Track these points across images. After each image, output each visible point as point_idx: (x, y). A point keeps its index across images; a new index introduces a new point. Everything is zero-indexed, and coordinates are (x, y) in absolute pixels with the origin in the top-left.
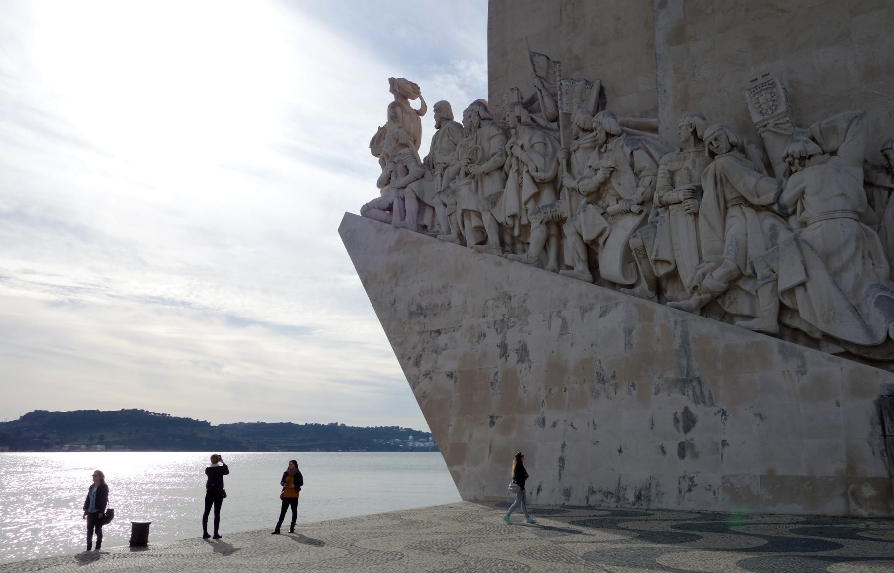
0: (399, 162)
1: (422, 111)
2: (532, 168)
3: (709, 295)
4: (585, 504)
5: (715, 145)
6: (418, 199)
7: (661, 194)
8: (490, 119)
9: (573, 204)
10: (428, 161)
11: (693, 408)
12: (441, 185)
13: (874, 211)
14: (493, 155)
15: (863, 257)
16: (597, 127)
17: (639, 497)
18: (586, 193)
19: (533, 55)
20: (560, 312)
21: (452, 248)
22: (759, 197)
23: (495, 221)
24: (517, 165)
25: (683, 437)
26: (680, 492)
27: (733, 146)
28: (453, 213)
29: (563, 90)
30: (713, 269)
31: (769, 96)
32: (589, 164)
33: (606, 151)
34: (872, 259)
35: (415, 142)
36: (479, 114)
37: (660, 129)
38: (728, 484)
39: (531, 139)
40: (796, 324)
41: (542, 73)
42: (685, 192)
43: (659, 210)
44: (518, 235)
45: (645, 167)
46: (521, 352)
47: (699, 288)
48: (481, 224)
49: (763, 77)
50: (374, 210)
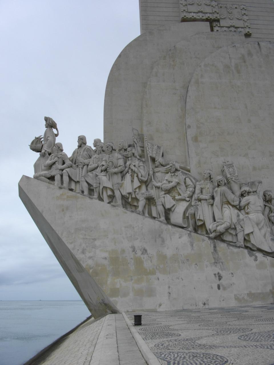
0: (60, 158)
1: (57, 135)
2: (140, 175)
4: (182, 309)
5: (221, 183)
6: (69, 177)
10: (72, 160)
11: (221, 272)
12: (82, 172)
14: (120, 166)
17: (204, 304)
18: (165, 190)
19: (133, 129)
20: (160, 235)
22: (233, 202)
24: (131, 172)
25: (218, 282)
26: (220, 301)
28: (98, 187)
29: (149, 147)
30: (221, 225)
33: (174, 176)
36: (112, 147)
37: (191, 171)
38: (237, 297)
39: (139, 164)
40: (248, 245)
43: (197, 201)
45: (190, 184)
47: (216, 231)
50: (42, 177)
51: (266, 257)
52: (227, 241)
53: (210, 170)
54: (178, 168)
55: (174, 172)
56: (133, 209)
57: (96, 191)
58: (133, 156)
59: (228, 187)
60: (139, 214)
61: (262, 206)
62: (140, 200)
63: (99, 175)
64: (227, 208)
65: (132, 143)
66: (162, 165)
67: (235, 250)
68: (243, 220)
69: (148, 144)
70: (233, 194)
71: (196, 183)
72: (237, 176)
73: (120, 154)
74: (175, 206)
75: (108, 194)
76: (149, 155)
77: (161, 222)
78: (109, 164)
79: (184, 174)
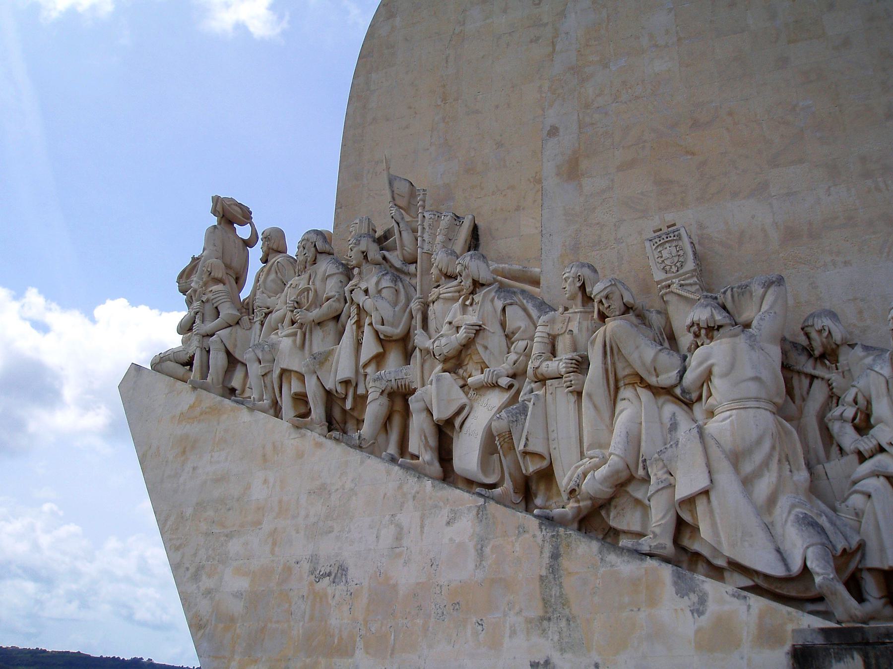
0: (208, 300)
3: (588, 503)
6: (228, 353)
8: (330, 254)
13: (794, 402)
14: (328, 299)
15: (779, 461)
16: (462, 273)
21: (266, 420)
23: (321, 388)
27: (628, 309)
28: (269, 372)
29: (426, 224)
30: (597, 467)
33: (471, 304)
34: (789, 464)
35: (237, 280)
36: (315, 245)
39: (377, 283)
40: (696, 547)
41: (402, 202)
43: (533, 385)
44: (350, 409)
45: (520, 328)
46: (337, 568)
47: (577, 493)
48: (304, 391)
51: (745, 597)
52: (624, 532)
55: (473, 293)
61: (765, 375)
67: (627, 567)
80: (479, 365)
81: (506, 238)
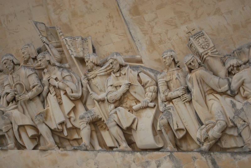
2: (69, 91)
3: (214, 141)
7: (166, 94)
9: (104, 110)
14: (34, 87)
16: (113, 62)
18: (114, 101)
19: (36, 23)
22: (220, 88)
28: (10, 129)
29: (69, 44)
30: (213, 127)
31: (204, 40)
32: (109, 84)
33: (120, 76)
36: (13, 61)
37: (144, 61)
42: (182, 91)
43: (166, 103)
45: (148, 81)
49: (192, 30)
52: (229, 149)
53: (171, 51)
54: (123, 62)
56: (75, 144)
57: (9, 137)
58: (49, 66)
59: (205, 68)
60: (86, 150)
62: (81, 129)
63: (6, 111)
64: (213, 99)
65: (41, 45)
66: (97, 65)
68: (242, 109)
69: (66, 40)
70: (216, 77)
71: (156, 78)
72: (214, 46)
73: (28, 67)
74: (136, 120)
75: (30, 135)
76: (72, 56)
77: (123, 151)
78: (15, 89)
79: (135, 69)
80: (133, 101)
81: (107, 45)
